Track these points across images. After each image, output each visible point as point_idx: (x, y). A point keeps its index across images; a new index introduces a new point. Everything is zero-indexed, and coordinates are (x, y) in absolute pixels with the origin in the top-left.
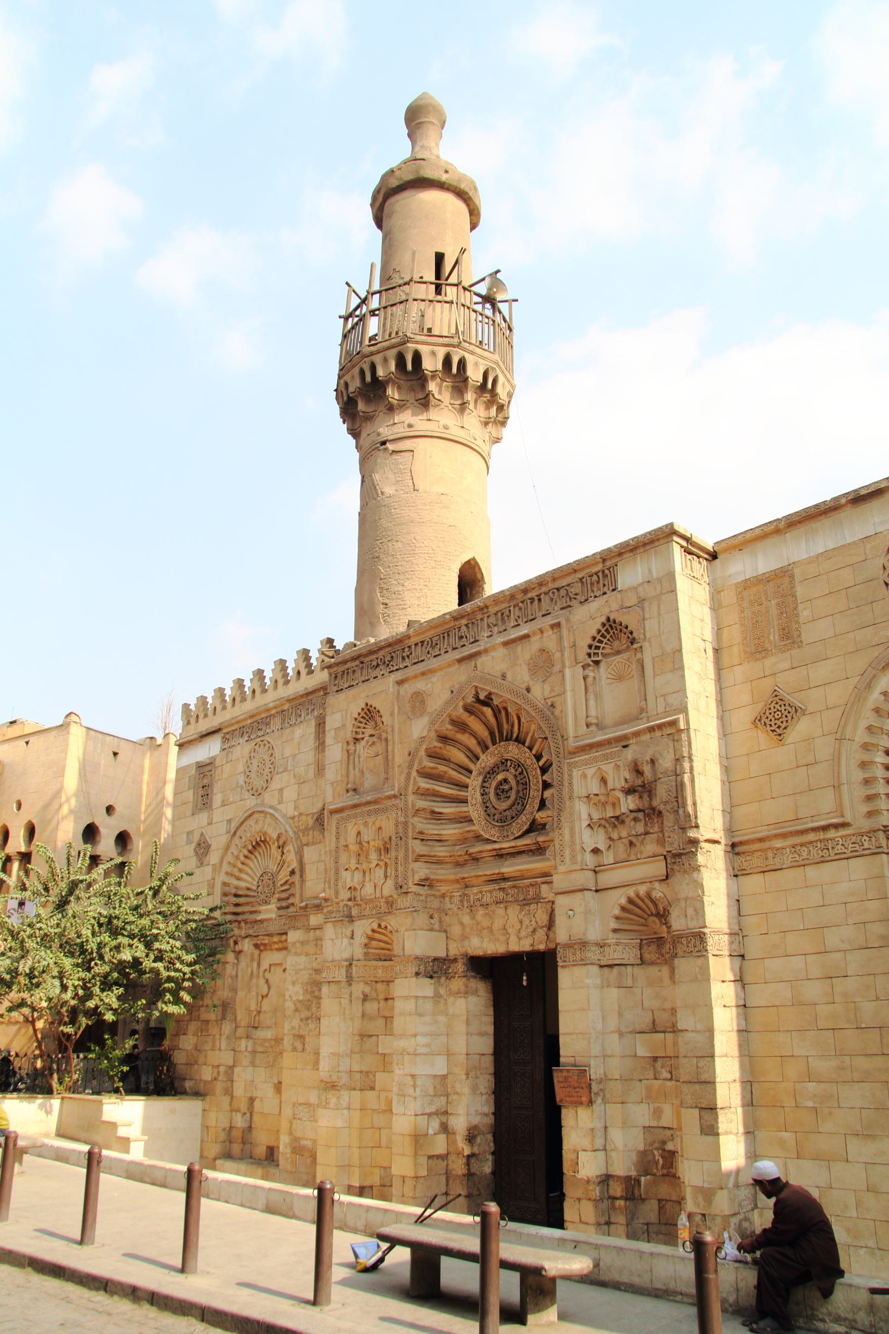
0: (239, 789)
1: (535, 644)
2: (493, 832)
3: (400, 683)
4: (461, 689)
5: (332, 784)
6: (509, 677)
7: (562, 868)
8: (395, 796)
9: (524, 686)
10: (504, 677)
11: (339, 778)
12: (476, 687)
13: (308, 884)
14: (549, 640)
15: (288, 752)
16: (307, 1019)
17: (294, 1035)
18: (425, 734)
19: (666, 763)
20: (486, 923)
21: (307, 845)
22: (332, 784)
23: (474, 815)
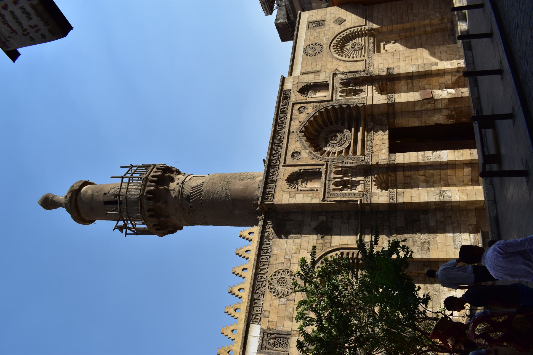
0: (288, 301)
1: (295, 112)
2: (347, 142)
3: (285, 162)
4: (299, 137)
5: (312, 198)
6: (302, 120)
7: (365, 102)
8: (327, 165)
9: (307, 115)
10: (300, 122)
11: (310, 195)
12: (300, 132)
13: (349, 243)
14: (296, 107)
15: (281, 259)
16: (413, 241)
17: (422, 250)
18: (307, 151)
19: (343, 77)
20: (378, 147)
21: (331, 243)
22: (312, 198)
23: (340, 149)
